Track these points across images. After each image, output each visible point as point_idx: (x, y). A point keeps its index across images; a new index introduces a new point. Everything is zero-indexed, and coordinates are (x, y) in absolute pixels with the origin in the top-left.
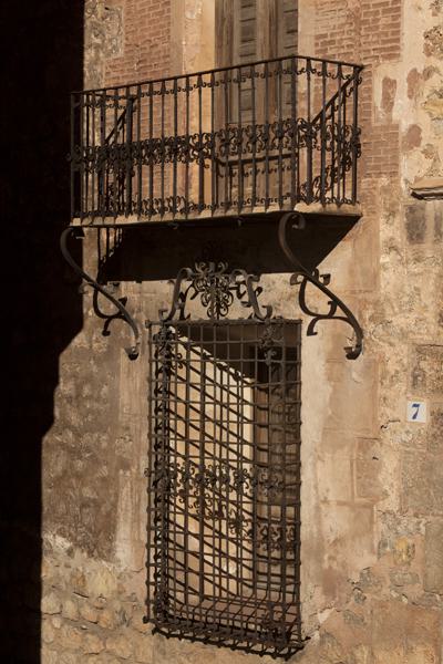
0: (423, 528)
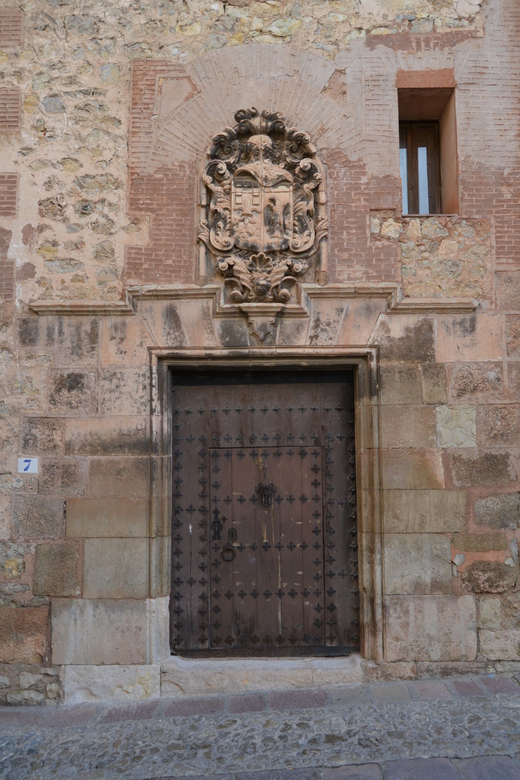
0: (33, 550)
